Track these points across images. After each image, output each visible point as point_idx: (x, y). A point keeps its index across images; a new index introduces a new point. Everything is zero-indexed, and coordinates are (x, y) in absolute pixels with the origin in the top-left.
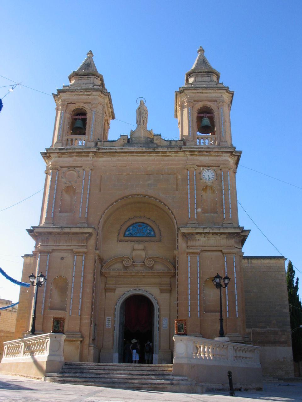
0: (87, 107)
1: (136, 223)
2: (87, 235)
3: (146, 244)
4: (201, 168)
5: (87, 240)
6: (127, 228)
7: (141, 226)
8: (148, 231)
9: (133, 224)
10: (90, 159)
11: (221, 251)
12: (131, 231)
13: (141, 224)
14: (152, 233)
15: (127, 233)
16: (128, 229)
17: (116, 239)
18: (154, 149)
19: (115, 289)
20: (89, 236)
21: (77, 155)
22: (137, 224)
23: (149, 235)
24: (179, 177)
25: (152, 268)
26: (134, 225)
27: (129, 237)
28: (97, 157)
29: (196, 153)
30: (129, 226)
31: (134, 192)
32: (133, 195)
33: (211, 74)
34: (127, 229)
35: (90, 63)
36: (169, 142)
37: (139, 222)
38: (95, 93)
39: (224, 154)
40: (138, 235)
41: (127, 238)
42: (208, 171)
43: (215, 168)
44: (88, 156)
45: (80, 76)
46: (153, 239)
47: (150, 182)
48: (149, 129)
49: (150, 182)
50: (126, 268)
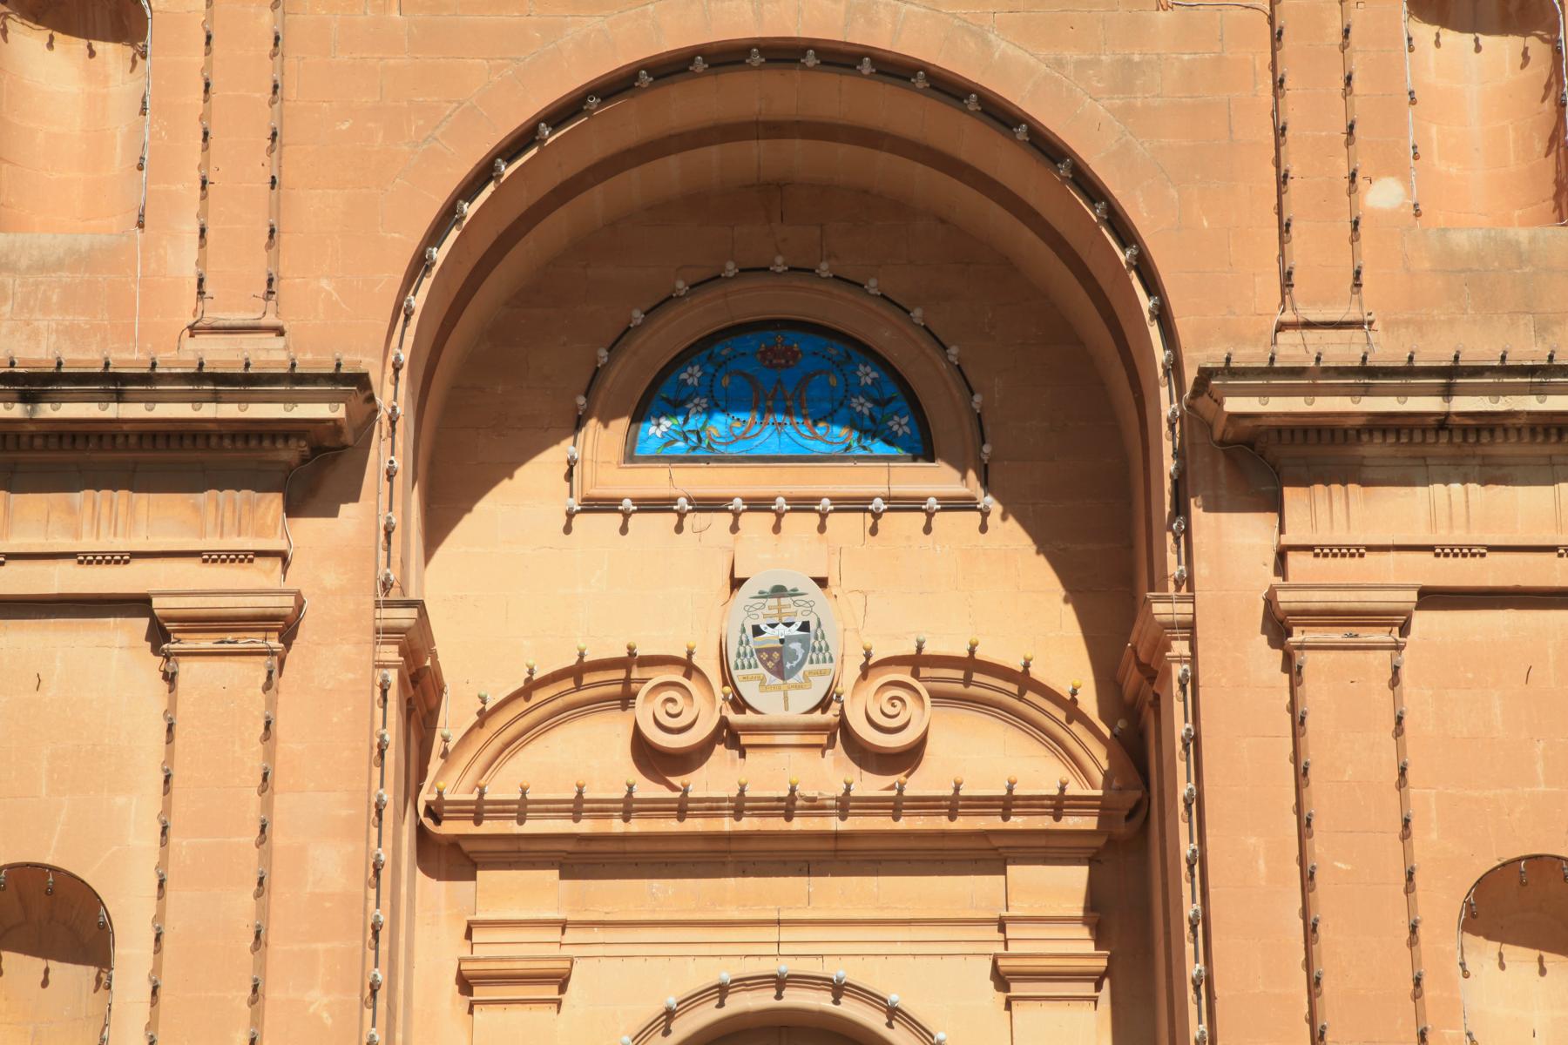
2: (289, 453)
19: (562, 981)
20: (304, 461)
22: (753, 342)
26: (722, 350)
50: (651, 759)
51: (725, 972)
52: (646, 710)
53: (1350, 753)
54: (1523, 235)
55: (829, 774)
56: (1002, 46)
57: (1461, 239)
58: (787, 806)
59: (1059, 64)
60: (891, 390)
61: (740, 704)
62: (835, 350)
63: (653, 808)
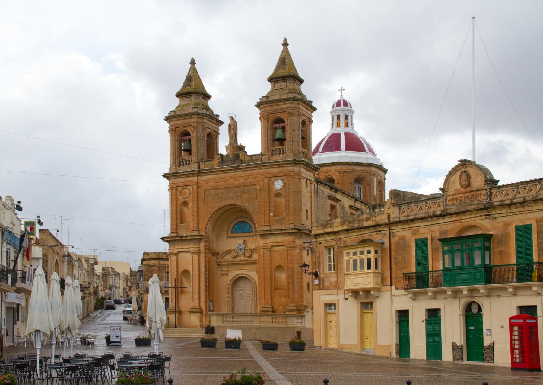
1: (239, 222)
3: (246, 239)
4: (273, 178)
5: (199, 242)
10: (195, 178)
15: (234, 230)
17: (226, 236)
24: (258, 188)
25: (250, 256)
28: (201, 176)
31: (228, 202)
32: (227, 205)
34: (234, 227)
38: (193, 116)
41: (233, 235)
43: (283, 177)
46: (251, 234)
47: (237, 194)
48: (239, 144)
51: (237, 273)
56: (246, 204)
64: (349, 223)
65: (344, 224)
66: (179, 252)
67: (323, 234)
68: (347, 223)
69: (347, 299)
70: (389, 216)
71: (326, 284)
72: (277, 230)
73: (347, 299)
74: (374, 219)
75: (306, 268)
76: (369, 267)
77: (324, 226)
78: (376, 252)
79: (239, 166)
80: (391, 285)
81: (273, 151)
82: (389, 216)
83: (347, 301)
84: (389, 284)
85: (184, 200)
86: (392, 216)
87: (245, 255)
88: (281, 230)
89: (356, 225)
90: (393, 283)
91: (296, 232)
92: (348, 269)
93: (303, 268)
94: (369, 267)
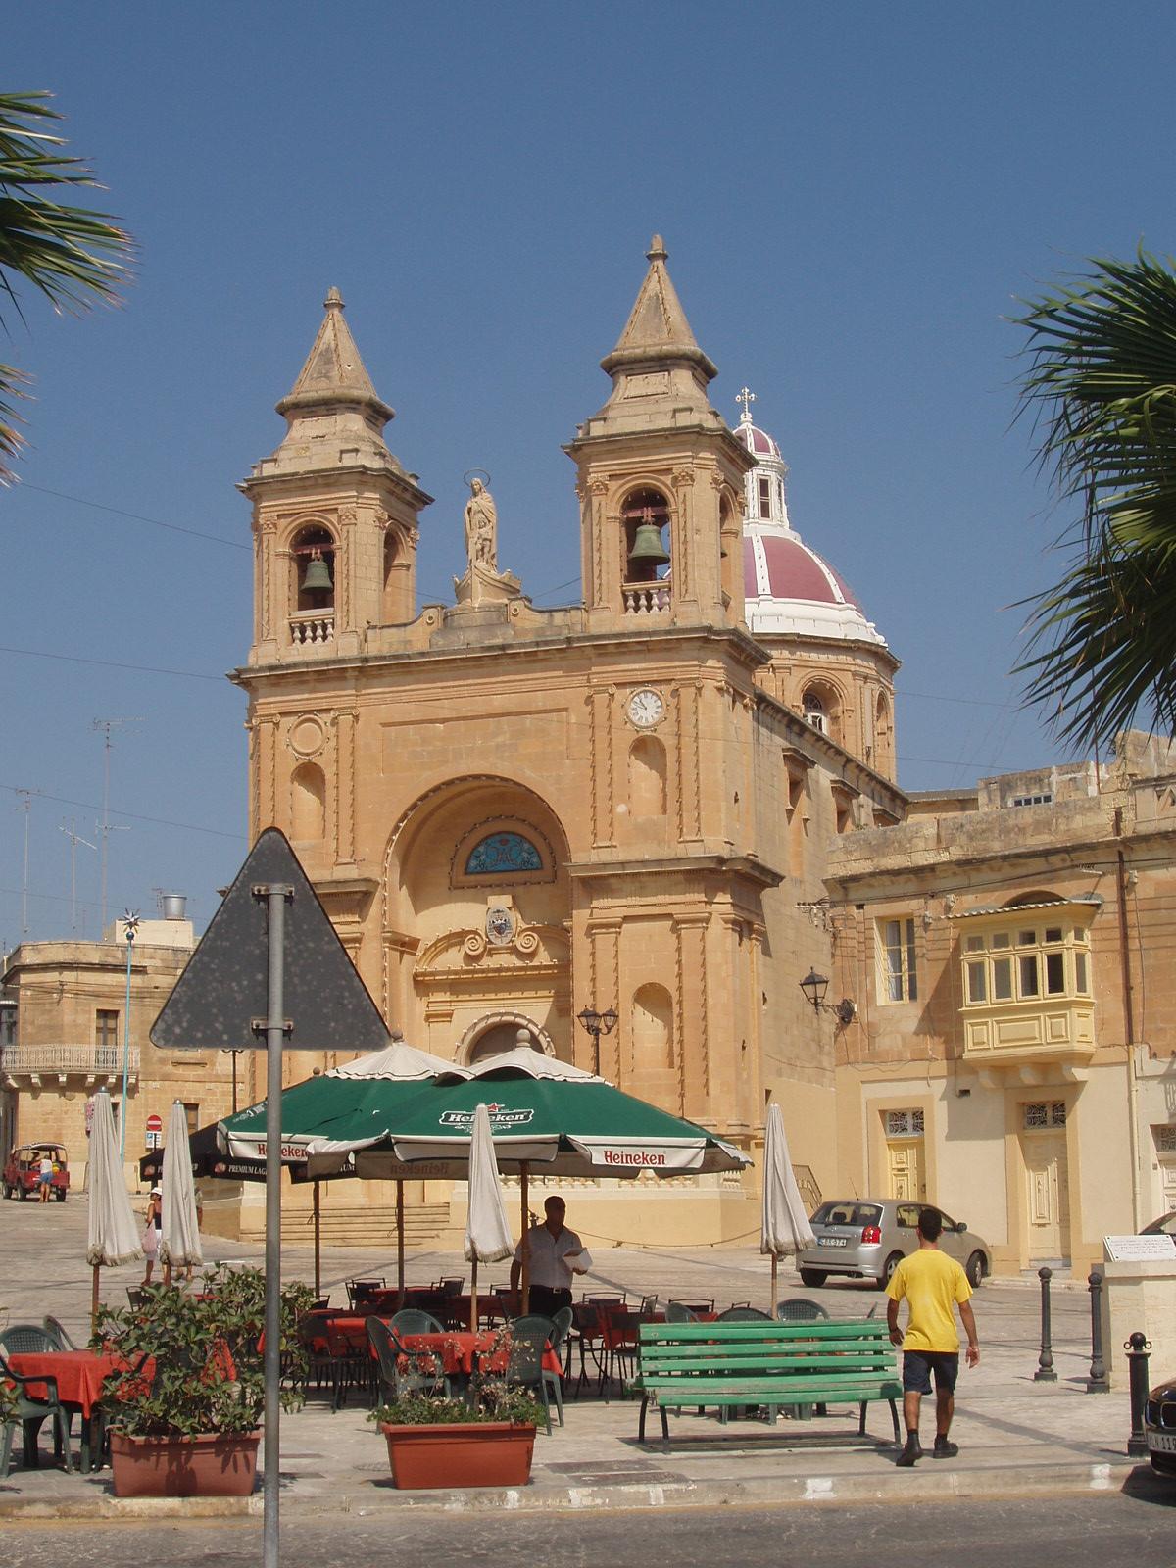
0: (331, 521)
1: (492, 835)
2: (357, 896)
6: (472, 853)
7: (507, 841)
8: (526, 855)
9: (487, 837)
11: (669, 916)
12: (482, 858)
13: (510, 837)
14: (535, 860)
15: (473, 863)
16: (476, 853)
18: (503, 647)
19: (450, 1015)
21: (315, 677)
22: (497, 838)
23: (526, 867)
26: (489, 841)
27: (478, 873)
29: (612, 649)
30: (479, 845)
33: (669, 362)
34: (473, 853)
35: (333, 346)
36: (546, 615)
37: (499, 833)
39: (685, 645)
40: (501, 867)
41: (472, 878)
42: (646, 697)
44: (345, 678)
45: (306, 409)
46: (537, 875)
47: (500, 739)
49: (500, 739)
52: (467, 946)
53: (605, 961)
54: (655, 818)
55: (513, 961)
56: (528, 773)
57: (640, 820)
58: (499, 970)
59: (542, 777)
60: (532, 849)
61: (490, 942)
62: (518, 839)
63: (467, 972)
64: (971, 838)
65: (952, 841)
66: (626, 919)
67: (873, 875)
68: (963, 839)
69: (966, 1092)
70: (1119, 815)
71: (885, 1042)
72: (643, 863)
73: (966, 1092)
74: (1062, 827)
75: (820, 988)
76: (1056, 984)
77: (877, 849)
78: (1029, 938)
79: (510, 646)
80: (1130, 1041)
81: (624, 594)
82: (1119, 815)
83: (965, 1098)
84: (1123, 1041)
85: (304, 760)
86: (1127, 816)
87: (514, 950)
88: (660, 862)
89: (997, 847)
90: (1137, 1036)
91: (711, 871)
92: (978, 992)
93: (809, 989)
94: (1056, 984)
